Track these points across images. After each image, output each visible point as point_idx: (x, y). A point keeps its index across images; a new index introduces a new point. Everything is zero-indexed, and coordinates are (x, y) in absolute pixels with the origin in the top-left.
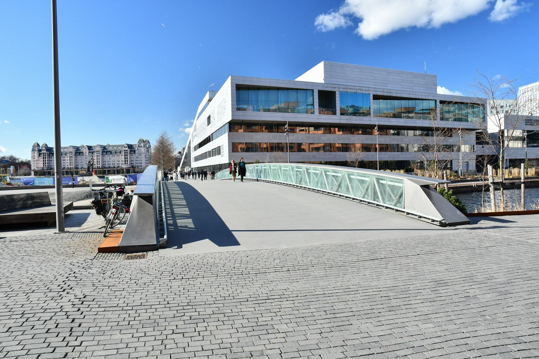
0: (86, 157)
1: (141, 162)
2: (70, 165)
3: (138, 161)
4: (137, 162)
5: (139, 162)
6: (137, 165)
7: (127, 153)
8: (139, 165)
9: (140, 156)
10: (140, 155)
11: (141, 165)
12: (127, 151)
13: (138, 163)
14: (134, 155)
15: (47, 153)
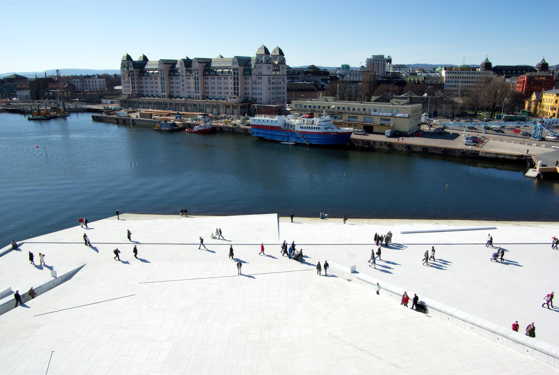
0: (183, 79)
1: (260, 91)
2: (162, 92)
3: (256, 89)
4: (254, 91)
5: (257, 91)
6: (254, 96)
7: (238, 74)
8: (257, 96)
9: (260, 81)
10: (259, 78)
11: (260, 96)
12: (237, 69)
13: (256, 94)
14: (250, 77)
15: (136, 71)
